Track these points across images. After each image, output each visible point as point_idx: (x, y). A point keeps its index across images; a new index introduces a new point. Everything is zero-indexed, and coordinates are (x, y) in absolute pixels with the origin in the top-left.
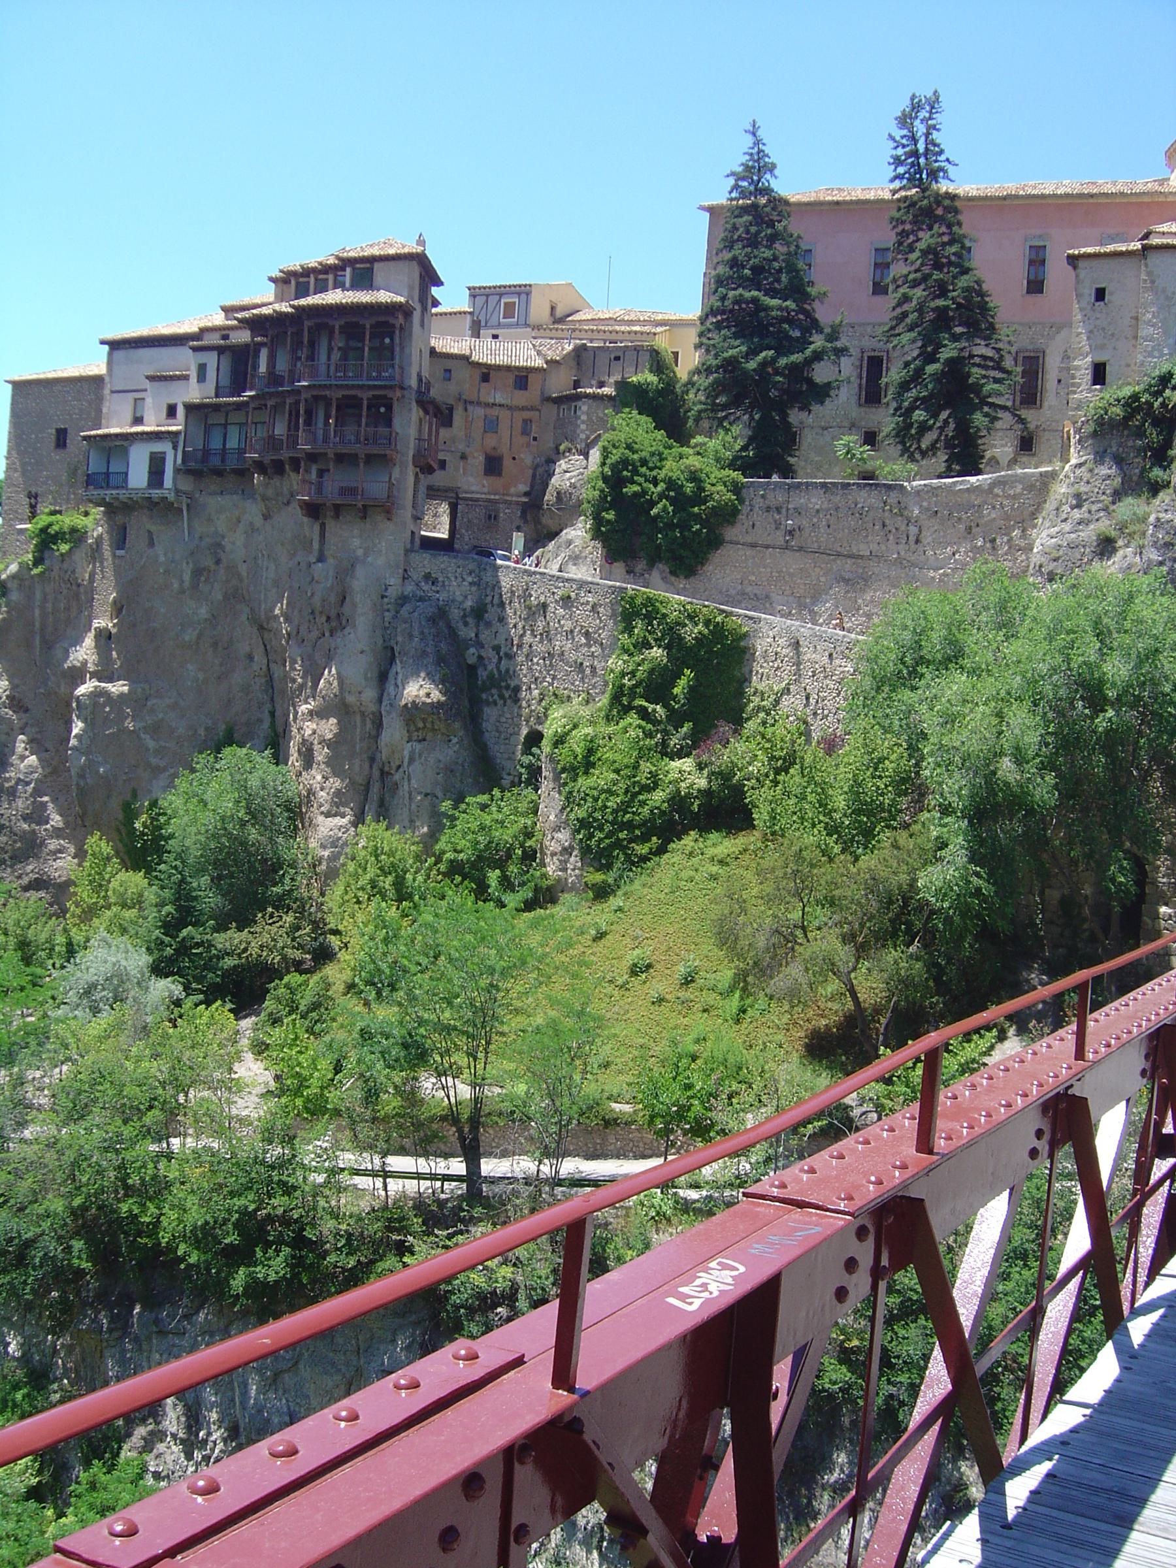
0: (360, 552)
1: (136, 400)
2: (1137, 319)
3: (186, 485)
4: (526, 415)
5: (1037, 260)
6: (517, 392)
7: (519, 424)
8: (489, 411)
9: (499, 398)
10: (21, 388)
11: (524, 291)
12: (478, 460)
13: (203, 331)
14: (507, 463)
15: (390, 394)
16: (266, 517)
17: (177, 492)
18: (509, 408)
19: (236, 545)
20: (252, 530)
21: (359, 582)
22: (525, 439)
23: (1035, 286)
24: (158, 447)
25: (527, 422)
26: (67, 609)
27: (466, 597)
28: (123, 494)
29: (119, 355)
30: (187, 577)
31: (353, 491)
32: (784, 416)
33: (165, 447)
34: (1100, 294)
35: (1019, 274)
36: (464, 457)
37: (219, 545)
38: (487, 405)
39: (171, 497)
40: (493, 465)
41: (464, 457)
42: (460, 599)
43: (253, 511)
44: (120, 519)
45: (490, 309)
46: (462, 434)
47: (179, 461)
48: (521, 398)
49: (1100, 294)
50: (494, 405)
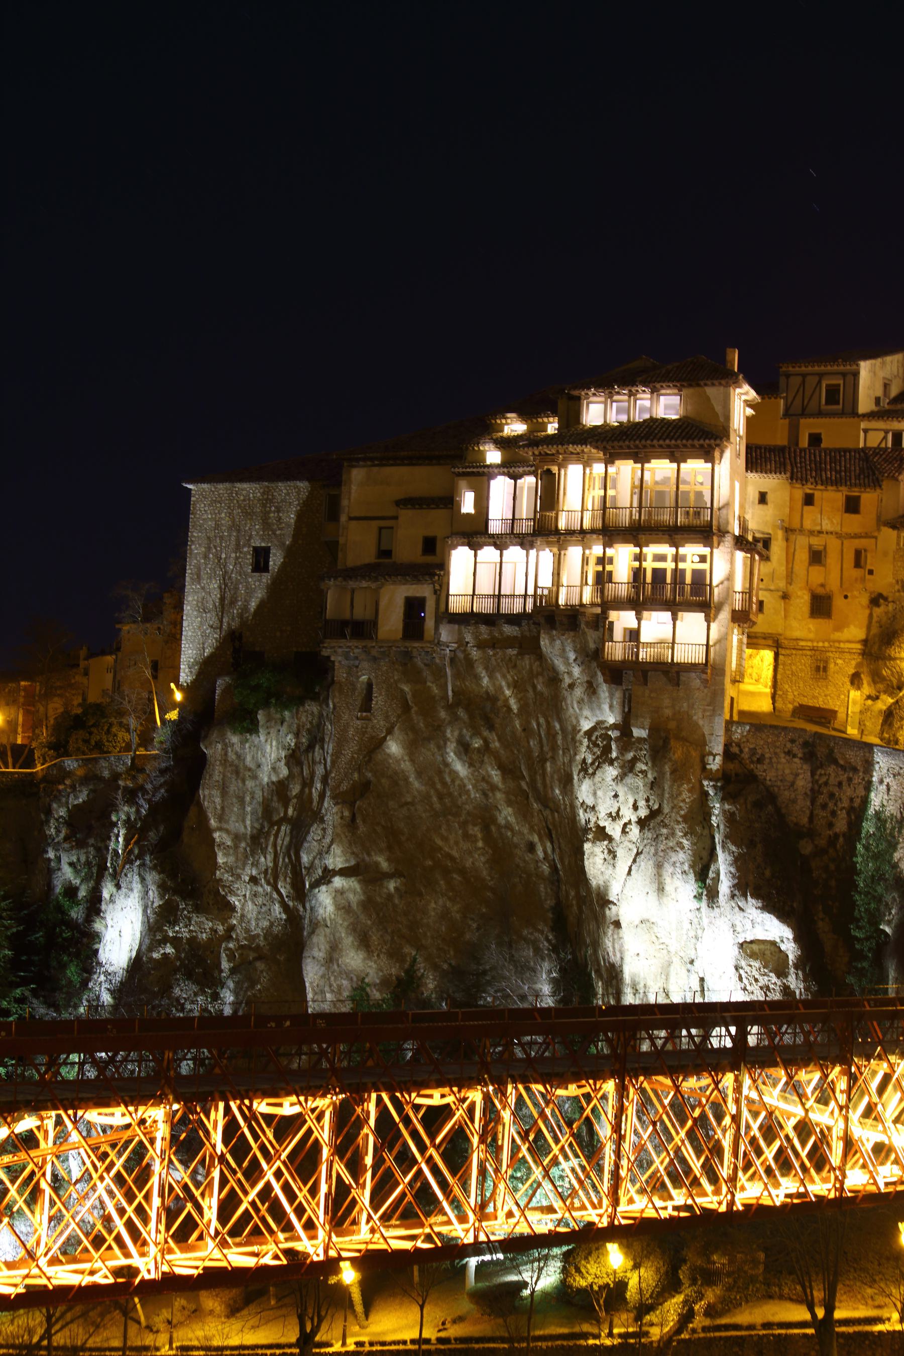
1: (380, 529)
6: (847, 515)
7: (850, 557)
9: (827, 526)
12: (802, 601)
14: (838, 602)
18: (839, 536)
22: (858, 573)
27: (797, 775)
38: (811, 533)
42: (790, 778)
45: (808, 394)
46: (782, 570)
50: (820, 532)
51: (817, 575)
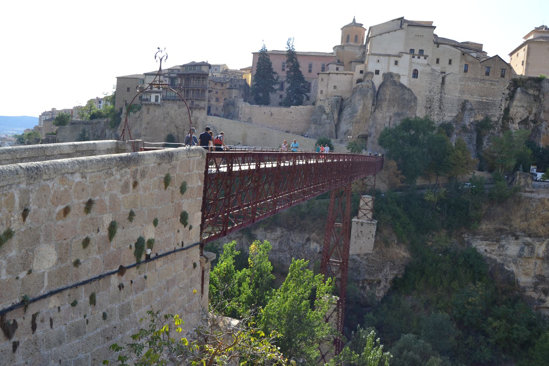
0: (199, 116)
2: (328, 84)
3: (162, 102)
4: (223, 91)
5: (310, 66)
7: (222, 92)
8: (216, 90)
9: (218, 88)
10: (119, 78)
11: (218, 66)
12: (214, 99)
13: (165, 73)
15: (205, 89)
16: (179, 108)
17: (161, 103)
19: (172, 112)
20: (175, 110)
21: (199, 121)
22: (222, 95)
23: (310, 71)
24: (157, 95)
25: (223, 92)
26: (135, 123)
28: (150, 103)
29: (147, 77)
30: (162, 118)
31: (198, 105)
32: (268, 94)
33: (159, 95)
34: (322, 79)
35: (307, 69)
36: (212, 98)
37: (168, 113)
38: (216, 89)
39: (160, 104)
40: (217, 100)
41: (212, 98)
43: (176, 107)
44: (148, 107)
47: (161, 97)
48: (222, 88)
49: (322, 79)
51: (217, 95)
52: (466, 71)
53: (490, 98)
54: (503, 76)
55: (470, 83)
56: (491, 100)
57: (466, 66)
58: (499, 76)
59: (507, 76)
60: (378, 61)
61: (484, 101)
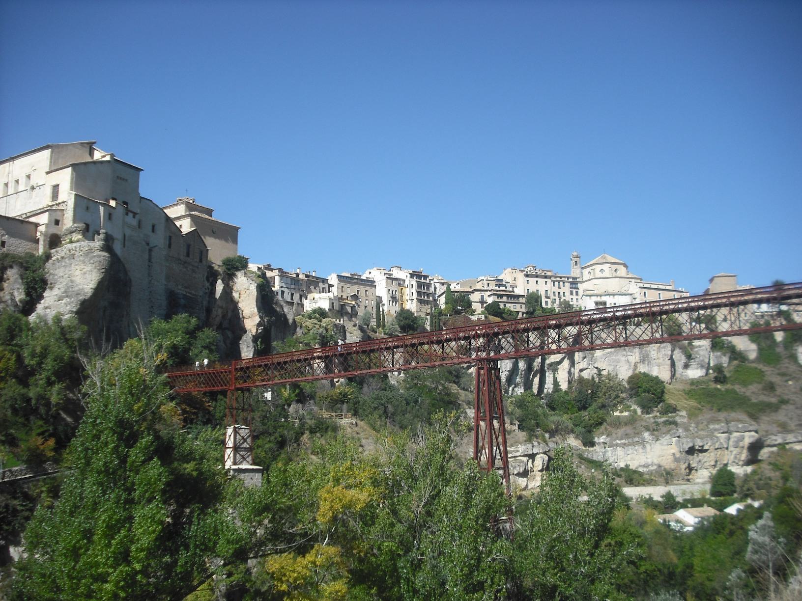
52: (170, 246)
53: (193, 292)
54: (201, 261)
55: (174, 265)
56: (194, 295)
57: (170, 237)
58: (198, 261)
59: (204, 262)
60: (88, 208)
61: (188, 294)
